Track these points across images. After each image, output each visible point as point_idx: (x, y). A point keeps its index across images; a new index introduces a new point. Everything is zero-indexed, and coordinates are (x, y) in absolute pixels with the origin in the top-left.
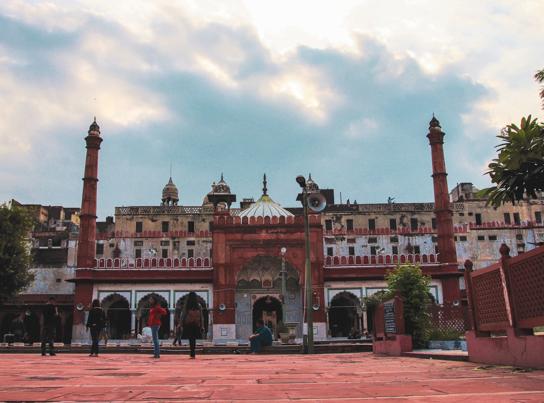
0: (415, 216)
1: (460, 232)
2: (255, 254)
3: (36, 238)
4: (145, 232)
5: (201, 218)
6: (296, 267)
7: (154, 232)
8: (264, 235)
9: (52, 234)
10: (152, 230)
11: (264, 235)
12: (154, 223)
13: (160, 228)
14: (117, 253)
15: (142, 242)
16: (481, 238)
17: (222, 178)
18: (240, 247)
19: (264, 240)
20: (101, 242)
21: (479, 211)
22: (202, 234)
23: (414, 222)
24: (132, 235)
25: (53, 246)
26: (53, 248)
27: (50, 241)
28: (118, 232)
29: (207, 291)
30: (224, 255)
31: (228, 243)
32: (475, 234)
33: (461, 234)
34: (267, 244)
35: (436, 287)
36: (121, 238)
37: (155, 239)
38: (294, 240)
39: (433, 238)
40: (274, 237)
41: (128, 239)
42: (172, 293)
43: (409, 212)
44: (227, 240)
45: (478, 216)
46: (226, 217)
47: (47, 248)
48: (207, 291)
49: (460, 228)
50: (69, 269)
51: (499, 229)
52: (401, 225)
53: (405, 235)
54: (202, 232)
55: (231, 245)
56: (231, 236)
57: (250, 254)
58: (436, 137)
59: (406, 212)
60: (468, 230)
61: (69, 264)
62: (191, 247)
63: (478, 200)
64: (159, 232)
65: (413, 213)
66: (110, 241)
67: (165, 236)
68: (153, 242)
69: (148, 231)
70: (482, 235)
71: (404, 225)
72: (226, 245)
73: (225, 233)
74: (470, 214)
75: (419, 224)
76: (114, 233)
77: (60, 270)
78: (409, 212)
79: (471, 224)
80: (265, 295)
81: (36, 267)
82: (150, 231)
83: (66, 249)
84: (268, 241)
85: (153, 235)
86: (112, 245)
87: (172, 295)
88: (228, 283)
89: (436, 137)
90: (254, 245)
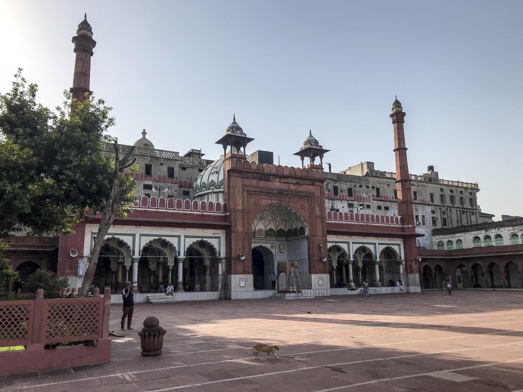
0: (337, 185)
1: (366, 201)
2: (270, 202)
5: (158, 161)
6: (304, 219)
8: (276, 184)
11: (276, 184)
16: (379, 208)
17: (234, 120)
18: (256, 194)
19: (277, 189)
21: (378, 186)
22: (160, 179)
23: (336, 189)
29: (218, 238)
30: (241, 201)
31: (245, 188)
32: (376, 204)
33: (367, 203)
34: (281, 193)
35: (399, 245)
38: (302, 192)
39: (348, 204)
40: (285, 187)
42: (182, 238)
43: (333, 180)
44: (243, 186)
45: (378, 189)
46: (243, 160)
48: (218, 238)
49: (366, 198)
51: (391, 202)
52: (327, 190)
53: (329, 199)
54: (159, 177)
55: (248, 191)
56: (247, 181)
57: (265, 202)
58: (398, 117)
59: (331, 180)
60: (372, 201)
62: (148, 191)
63: (379, 177)
65: (335, 181)
70: (380, 205)
71: (329, 191)
72: (243, 190)
73: (242, 178)
74: (373, 188)
75: (339, 191)
78: (333, 180)
79: (373, 196)
80: (259, 245)
84: (281, 190)
87: (182, 240)
88: (246, 230)
89: (398, 117)
90: (269, 193)
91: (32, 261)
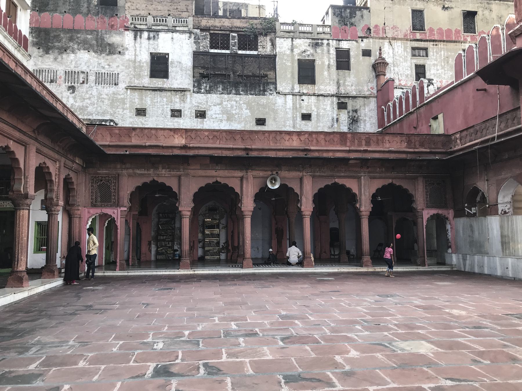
3: (202, 30)
4: (431, 30)
7: (449, 31)
9: (237, 23)
10: (445, 28)
12: (446, 12)
13: (459, 24)
14: (379, 67)
15: (426, 49)
20: (344, 45)
24: (406, 35)
25: (239, 49)
26: (240, 52)
27: (234, 37)
28: (376, 26)
36: (383, 38)
37: (451, 45)
41: (399, 43)
47: (228, 52)
50: (280, 100)
61: (280, 88)
64: (457, 32)
66: (364, 44)
67: (469, 39)
68: (448, 50)
69: (435, 28)
76: (369, 29)
77: (262, 100)
81: (208, 92)
82: (440, 29)
83: (271, 59)
85: (446, 39)
86: (367, 53)
91: (397, 183)
